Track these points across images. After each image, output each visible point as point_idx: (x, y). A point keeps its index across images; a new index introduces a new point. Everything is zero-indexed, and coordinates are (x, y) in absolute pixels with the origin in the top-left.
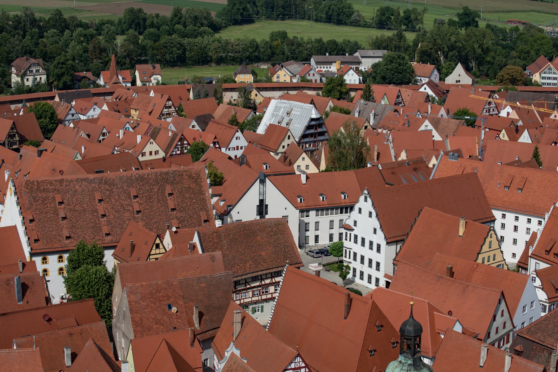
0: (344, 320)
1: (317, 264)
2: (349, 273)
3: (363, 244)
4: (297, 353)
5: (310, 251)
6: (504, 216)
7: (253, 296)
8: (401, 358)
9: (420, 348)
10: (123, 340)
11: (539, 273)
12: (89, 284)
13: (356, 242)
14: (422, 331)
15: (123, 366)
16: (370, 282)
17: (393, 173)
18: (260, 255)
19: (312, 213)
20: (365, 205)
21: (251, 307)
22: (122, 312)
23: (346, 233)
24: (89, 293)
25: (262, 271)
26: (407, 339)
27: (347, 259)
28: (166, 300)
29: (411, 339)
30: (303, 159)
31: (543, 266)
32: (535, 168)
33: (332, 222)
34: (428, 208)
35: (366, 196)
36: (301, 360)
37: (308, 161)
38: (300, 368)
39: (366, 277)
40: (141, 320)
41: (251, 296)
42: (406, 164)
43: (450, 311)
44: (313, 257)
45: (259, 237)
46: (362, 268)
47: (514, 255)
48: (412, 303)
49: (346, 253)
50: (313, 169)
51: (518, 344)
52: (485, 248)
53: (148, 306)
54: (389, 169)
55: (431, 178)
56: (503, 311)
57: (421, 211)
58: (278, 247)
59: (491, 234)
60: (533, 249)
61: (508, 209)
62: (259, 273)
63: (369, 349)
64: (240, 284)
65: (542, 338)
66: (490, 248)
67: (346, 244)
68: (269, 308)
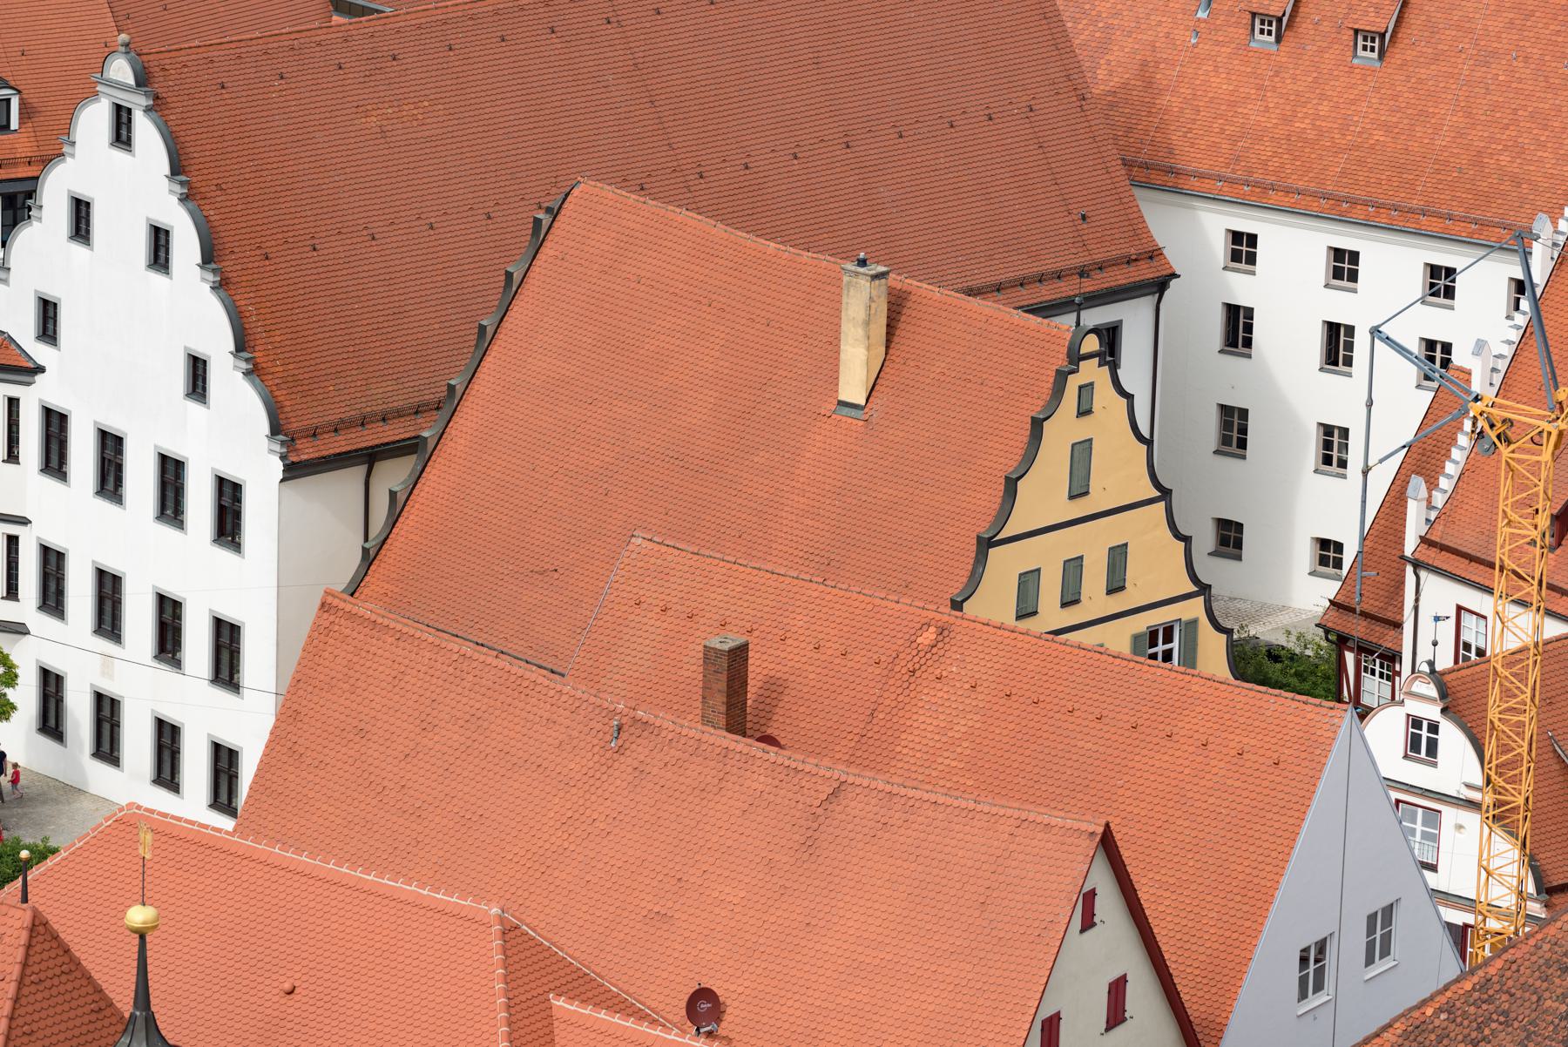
3: (110, 480)
6: (1243, 248)
13: (55, 462)
16: (167, 773)
31: (1512, 628)
34: (608, 192)
35: (126, 99)
39: (137, 742)
46: (107, 672)
47: (1328, 551)
48: (138, 915)
57: (554, 213)
59: (1086, 390)
60: (1439, 499)
61: (1274, 198)
66: (1078, 491)
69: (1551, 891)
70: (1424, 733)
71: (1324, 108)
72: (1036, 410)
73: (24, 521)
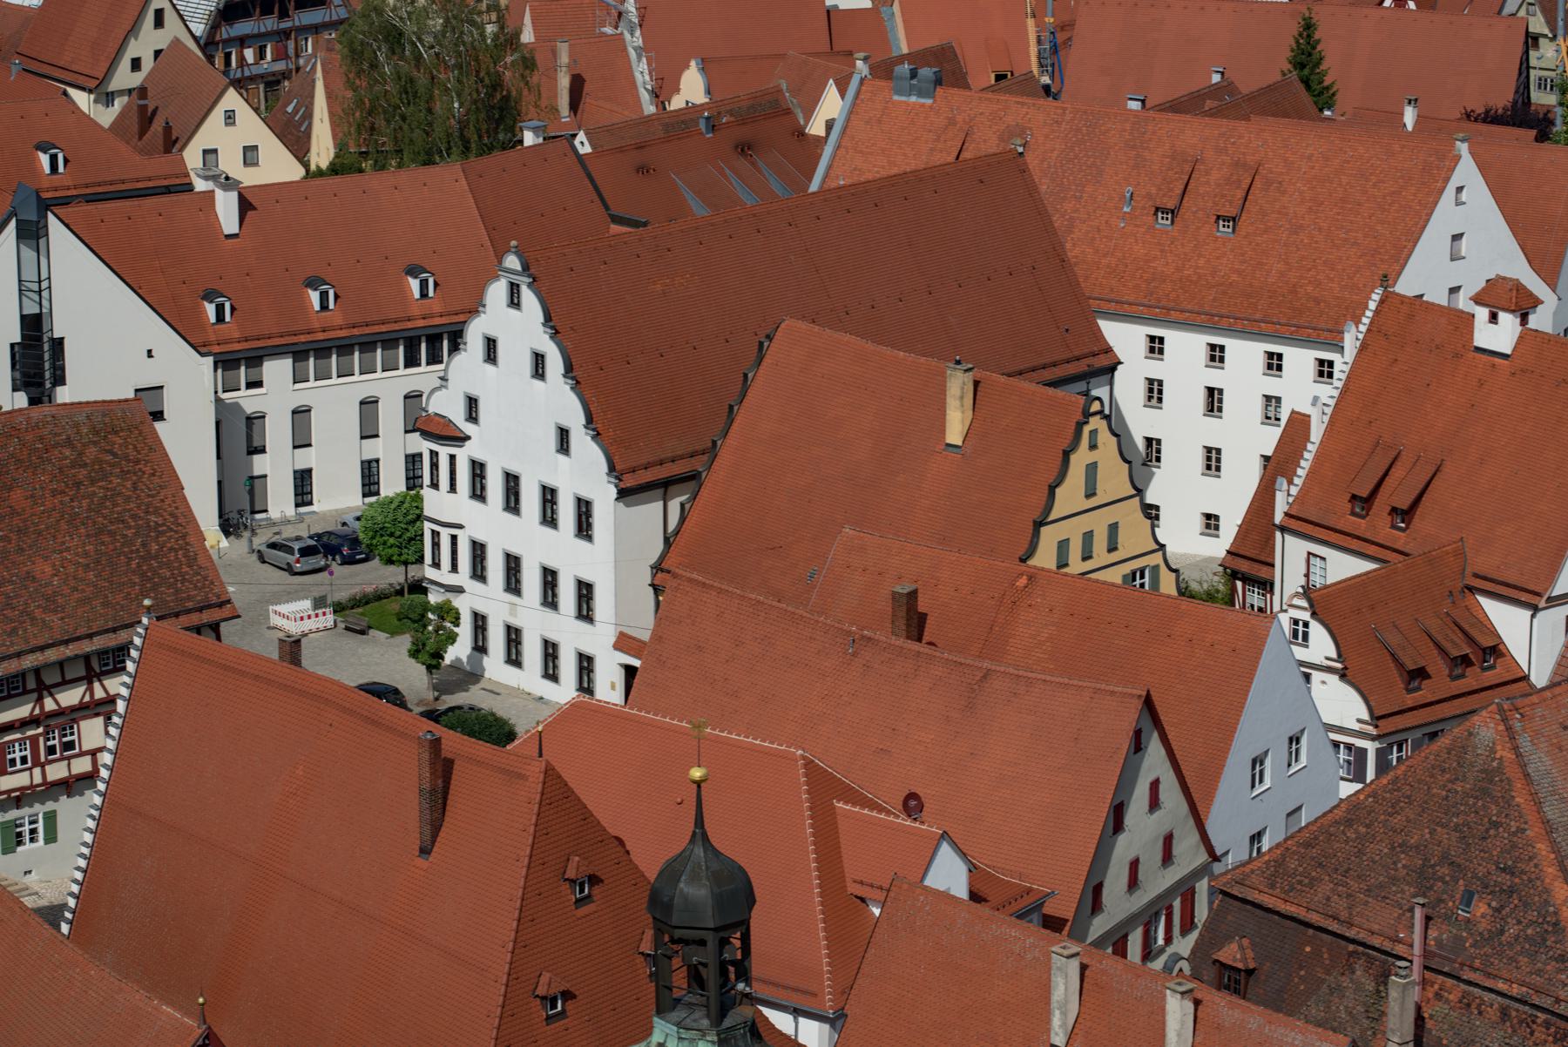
0: (421, 862)
1: (306, 605)
2: (452, 638)
3: (512, 502)
5: (273, 546)
6: (1156, 346)
9: (748, 982)
11: (1320, 602)
13: (478, 494)
14: (754, 902)
16: (551, 674)
17: (643, 170)
18: (30, 577)
19: (277, 370)
20: (512, 321)
23: (434, 455)
25: (42, 649)
26: (686, 942)
27: (443, 576)
29: (702, 943)
30: (230, 117)
31: (1342, 566)
32: (1300, 115)
33: (369, 405)
34: (803, 325)
37: (252, 128)
39: (532, 653)
42: (702, 125)
44: (289, 570)
45: (17, 495)
46: (513, 613)
47: (1211, 522)
48: (697, 773)
49: (436, 545)
50: (278, 166)
51: (1228, 938)
52: (1070, 496)
54: (621, 150)
55: (814, 186)
56: (1155, 785)
57: (769, 338)
58: (112, 534)
59: (1094, 433)
60: (1294, 491)
62: (29, 662)
63: (541, 991)
65: (1339, 905)
66: (1090, 494)
67: (436, 503)
68: (78, 817)
69: (1379, 718)
70: (1301, 628)
71: (1202, 262)
72: (1065, 445)
73: (460, 527)
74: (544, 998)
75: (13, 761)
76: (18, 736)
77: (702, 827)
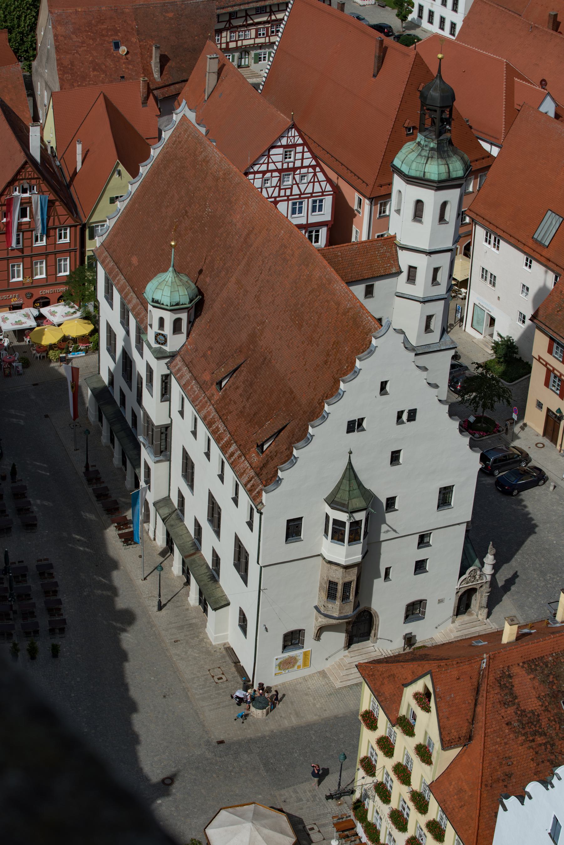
0: (373, 79)
2: (411, 12)
4: (290, 122)
7: (256, 37)
8: (420, 138)
9: (450, 125)
10: (46, 94)
12: (6, 8)
14: (453, 98)
15: (34, 133)
16: (442, 27)
21: (253, 53)
22: (46, 51)
24: (6, 21)
28: (112, 35)
29: (436, 111)
36: (297, 134)
38: (295, 146)
39: (437, 20)
40: (72, 63)
41: (253, 36)
43: (543, 80)
48: (440, 56)
53: (83, 43)
63: (406, 125)
64: (237, 18)
74: (406, 128)
75: (260, 34)
76: (263, 26)
77: (440, 73)
